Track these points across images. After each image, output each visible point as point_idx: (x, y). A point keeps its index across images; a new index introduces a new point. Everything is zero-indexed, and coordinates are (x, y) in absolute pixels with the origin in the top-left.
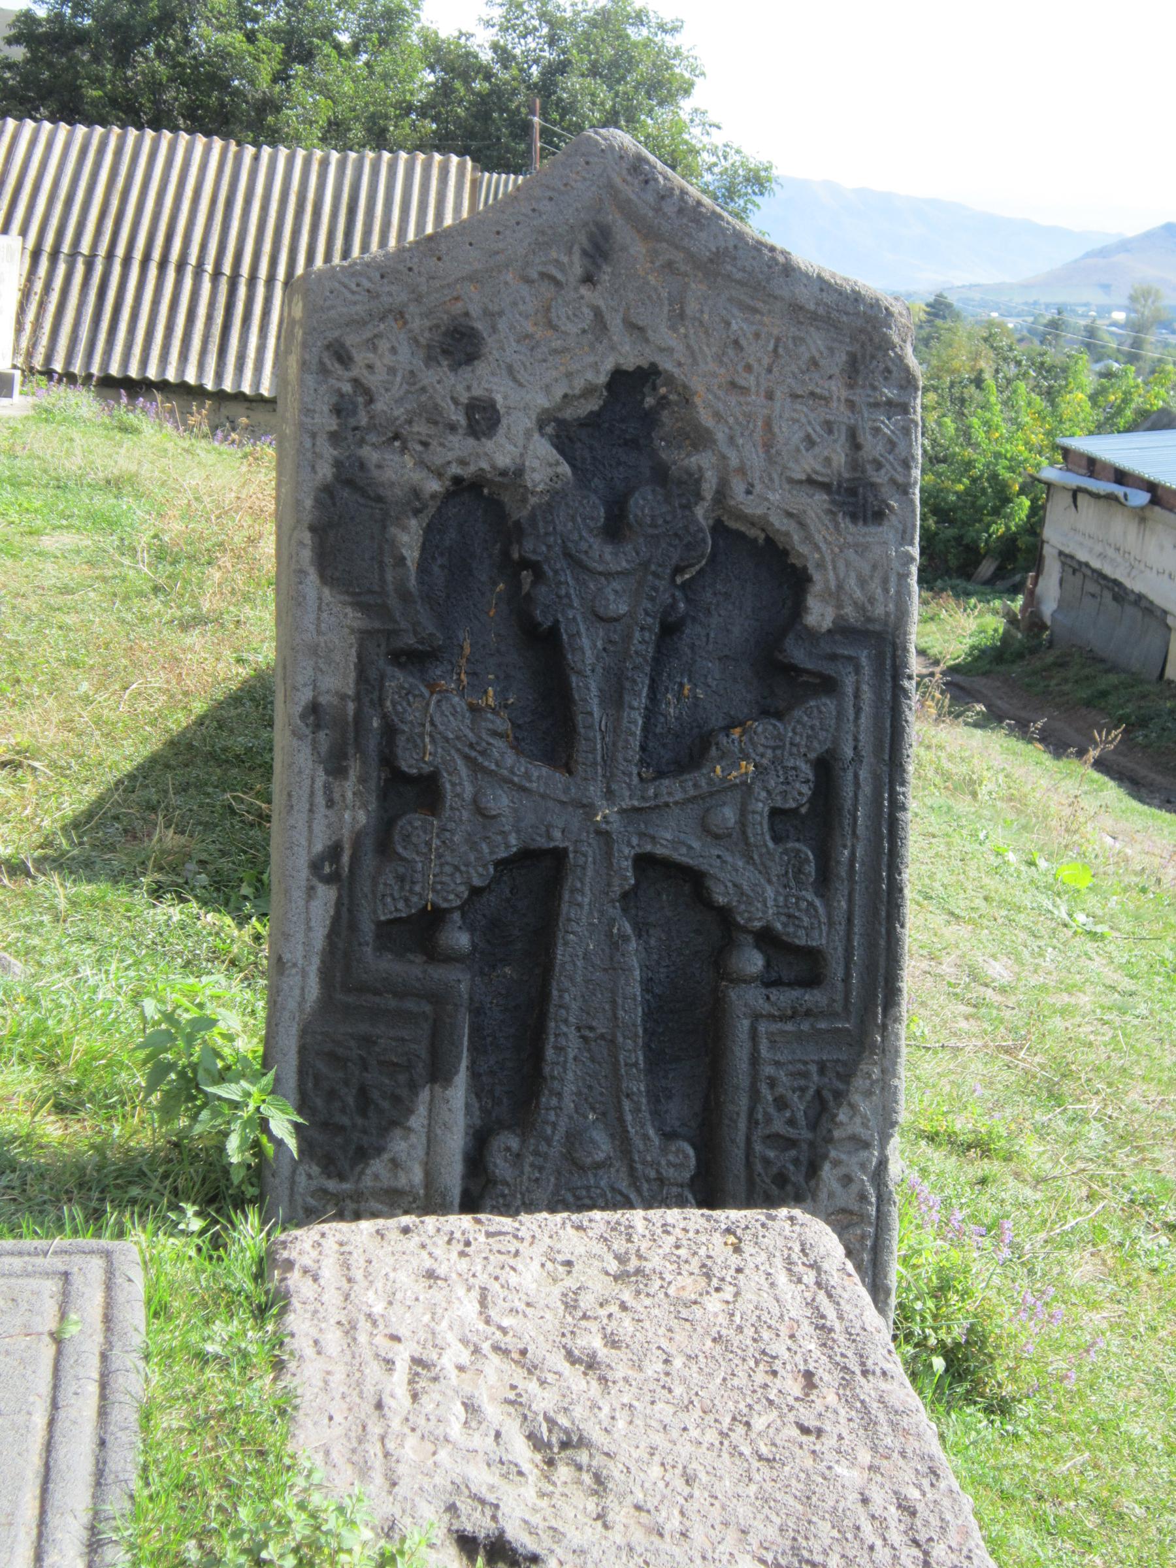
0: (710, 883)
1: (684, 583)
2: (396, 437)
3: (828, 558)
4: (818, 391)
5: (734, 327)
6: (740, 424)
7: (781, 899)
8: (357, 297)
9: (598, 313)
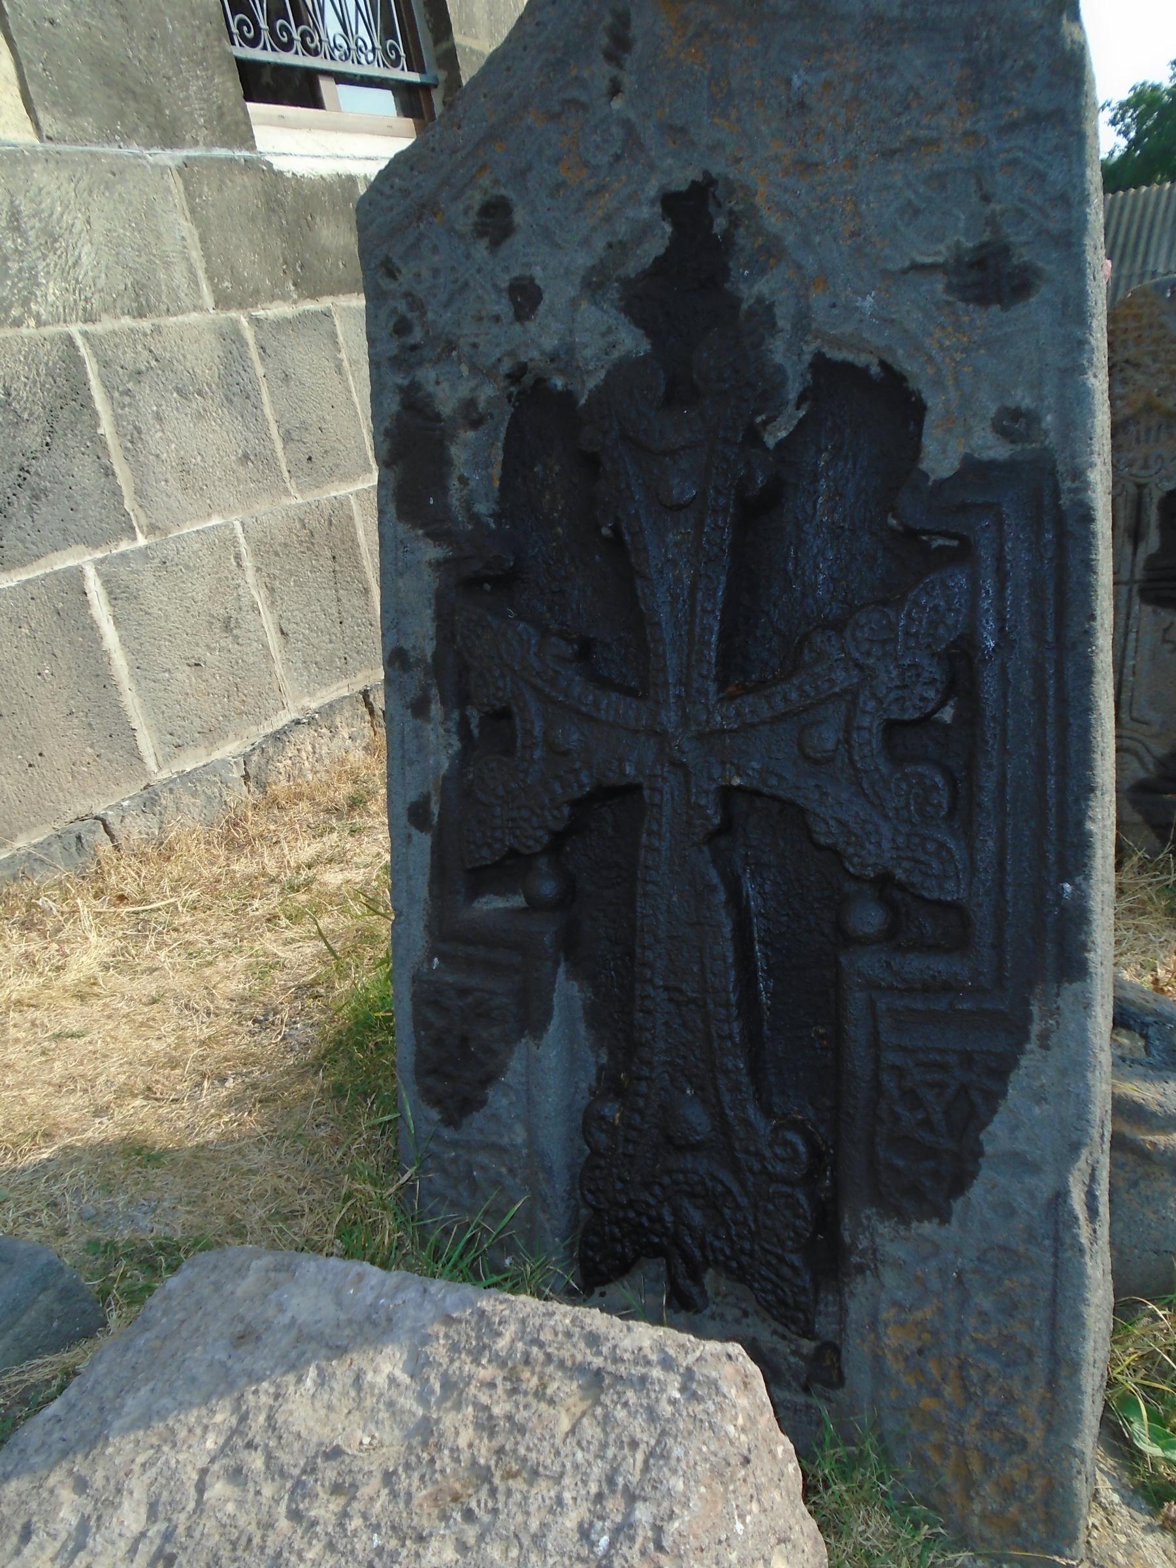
1: (780, 445)
4: (923, 133)
5: (796, 81)
7: (900, 840)
9: (628, 126)
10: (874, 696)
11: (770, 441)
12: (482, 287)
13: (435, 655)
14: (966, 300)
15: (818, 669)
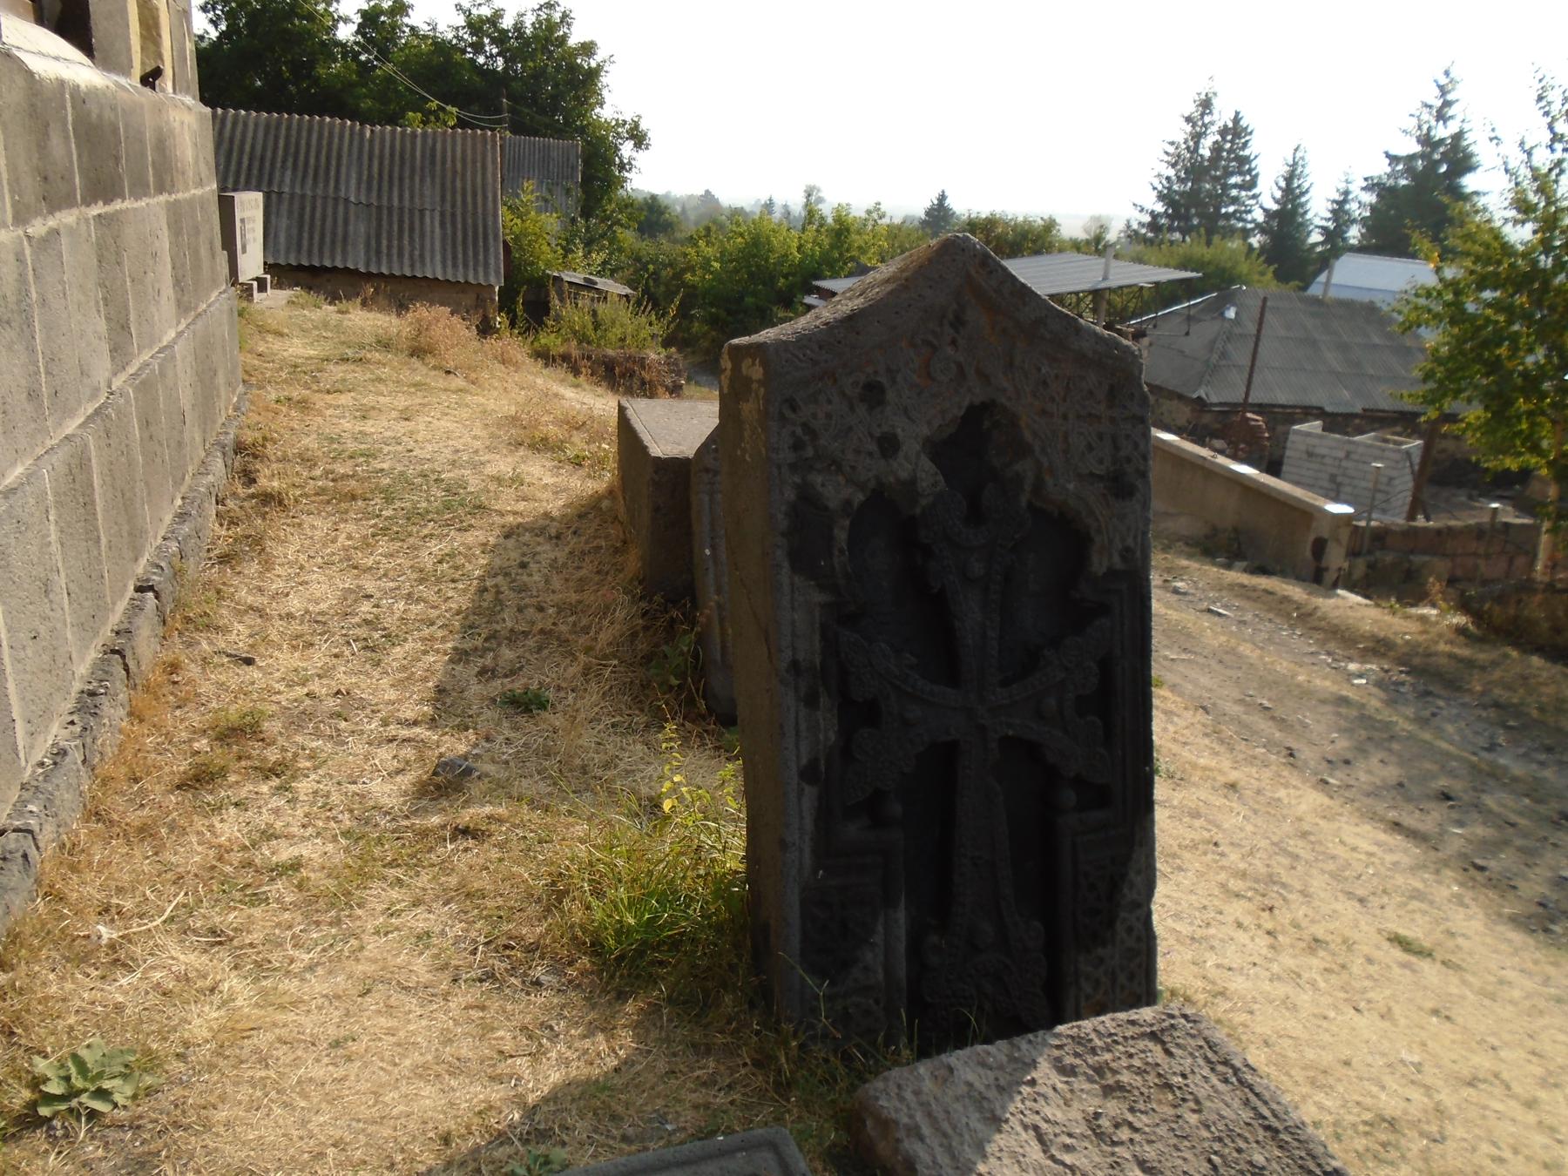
9: (960, 366)
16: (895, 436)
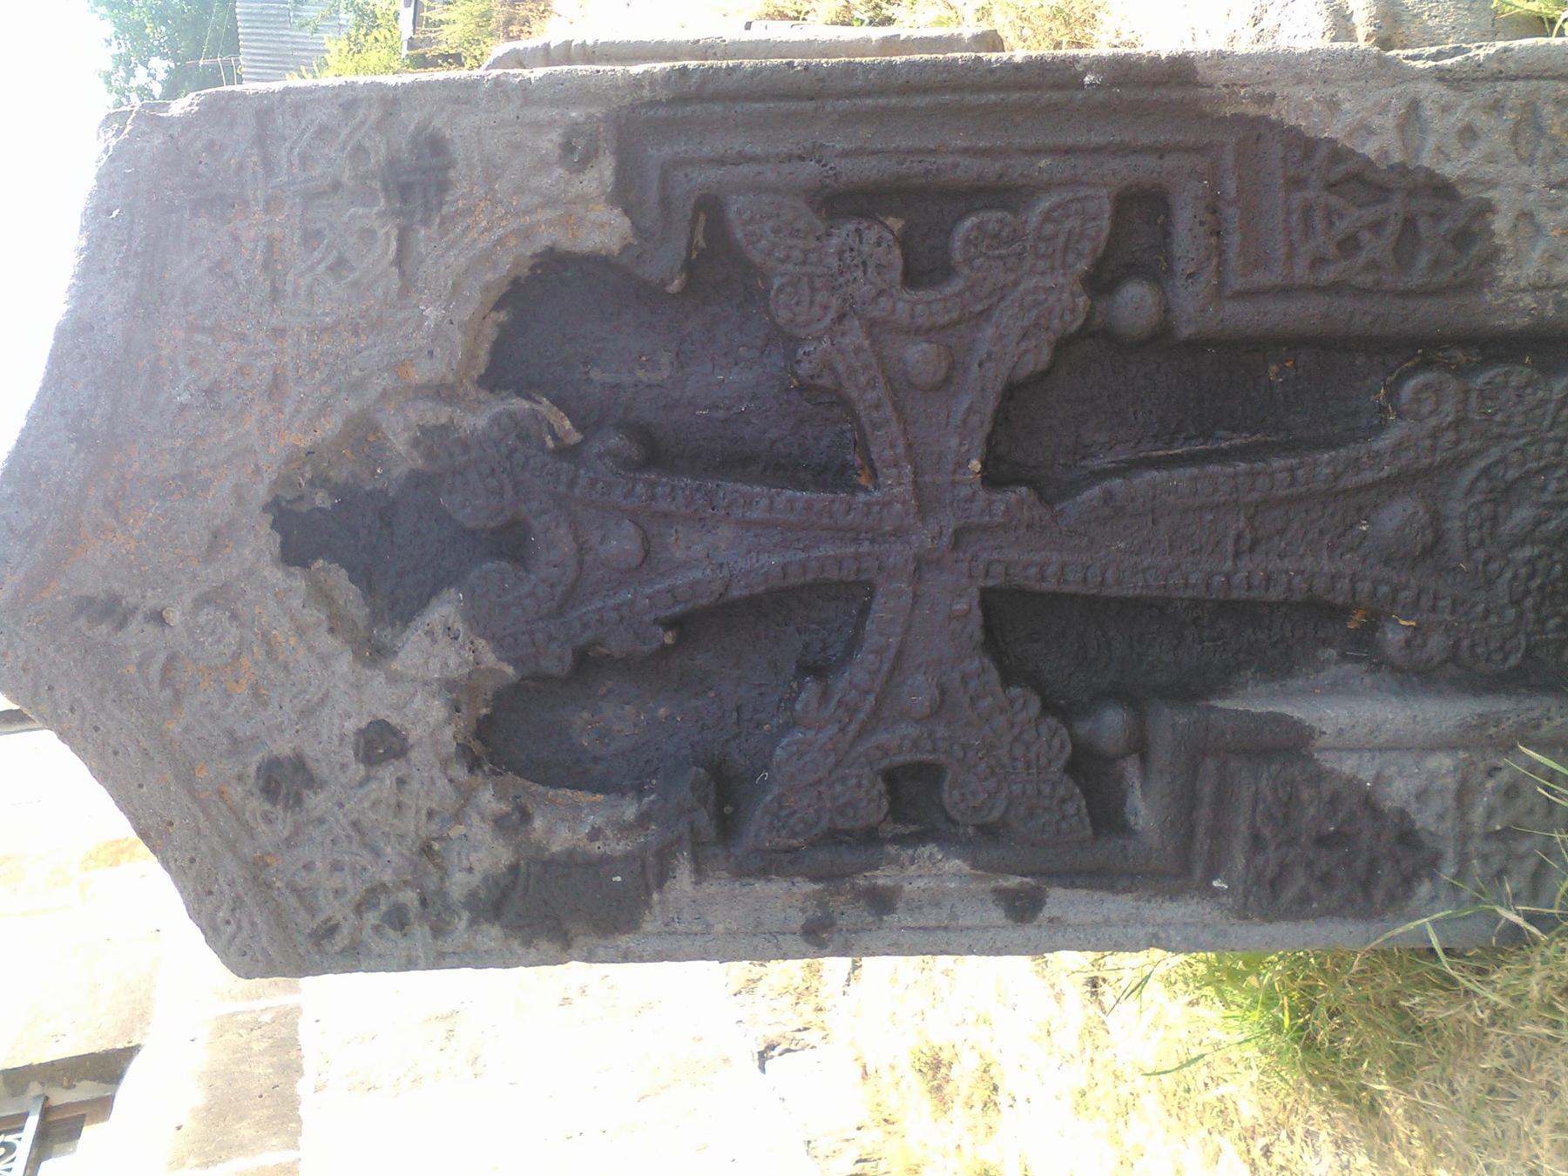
0: (1022, 373)
1: (579, 427)
2: (426, 850)
3: (513, 224)
5: (184, 398)
6: (330, 377)
7: (1041, 265)
8: (245, 923)
9: (201, 602)
10: (875, 299)
11: (576, 437)
12: (361, 801)
13: (815, 879)
14: (441, 204)
15: (841, 367)
16: (360, 732)
